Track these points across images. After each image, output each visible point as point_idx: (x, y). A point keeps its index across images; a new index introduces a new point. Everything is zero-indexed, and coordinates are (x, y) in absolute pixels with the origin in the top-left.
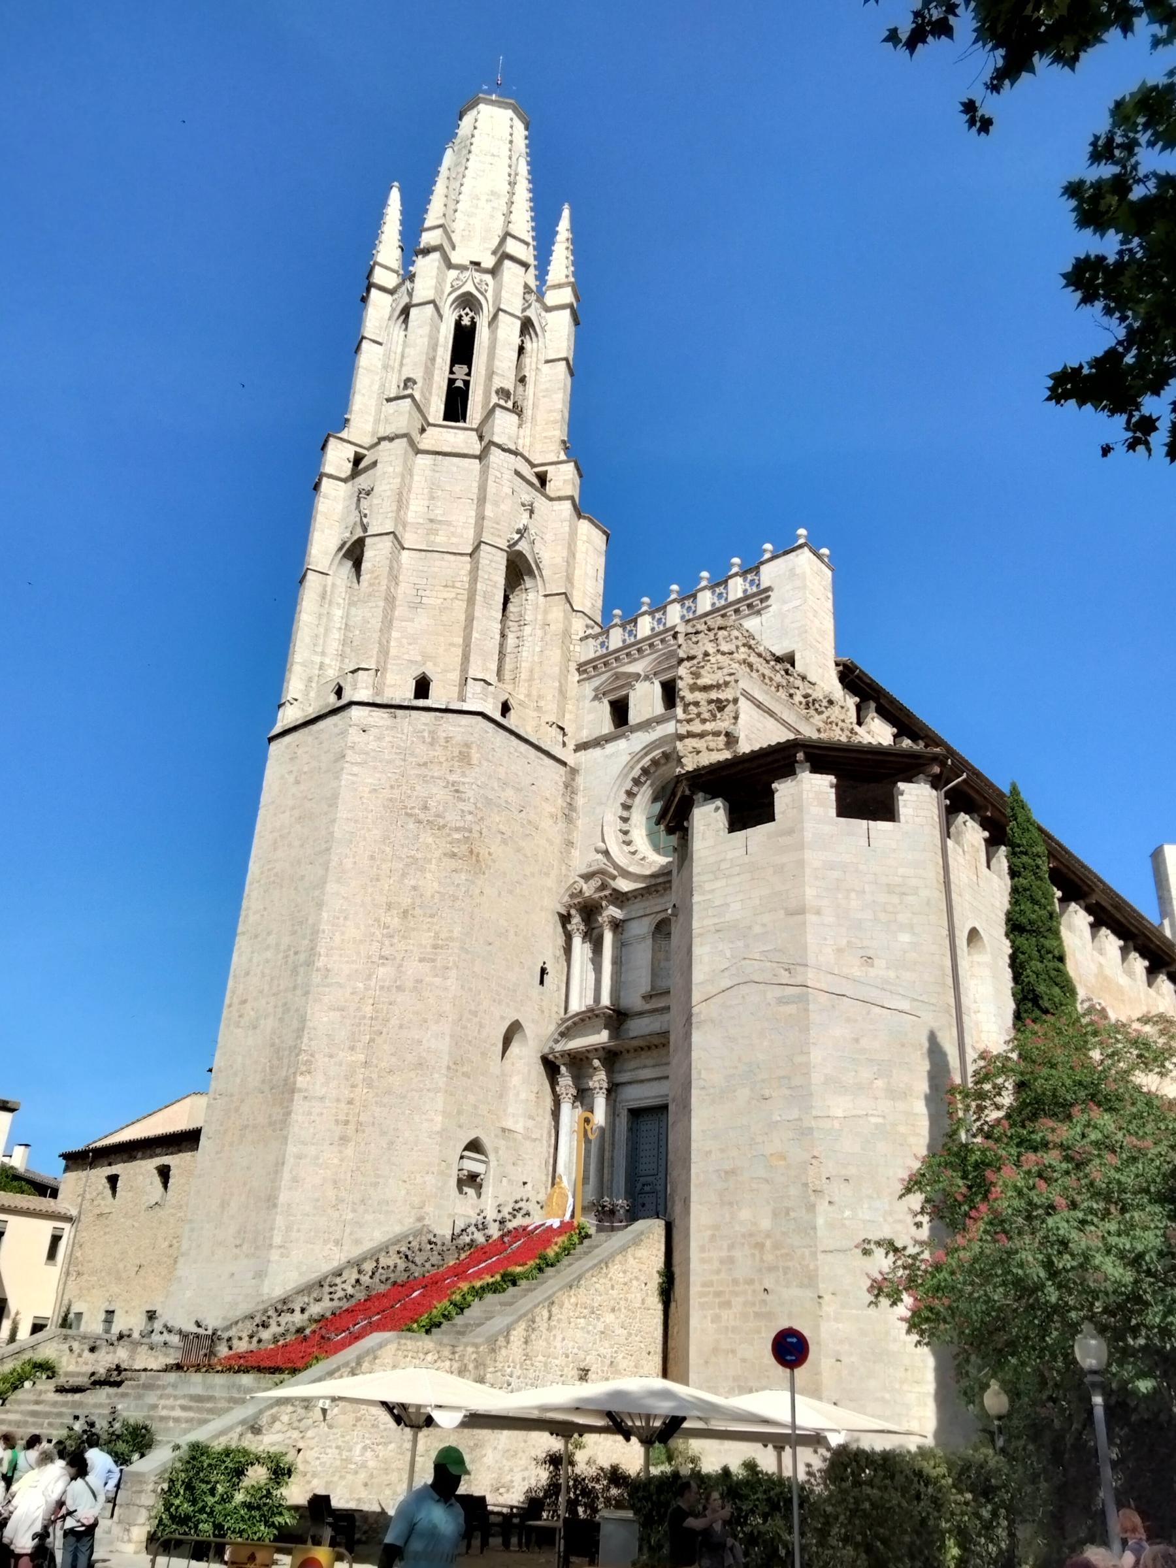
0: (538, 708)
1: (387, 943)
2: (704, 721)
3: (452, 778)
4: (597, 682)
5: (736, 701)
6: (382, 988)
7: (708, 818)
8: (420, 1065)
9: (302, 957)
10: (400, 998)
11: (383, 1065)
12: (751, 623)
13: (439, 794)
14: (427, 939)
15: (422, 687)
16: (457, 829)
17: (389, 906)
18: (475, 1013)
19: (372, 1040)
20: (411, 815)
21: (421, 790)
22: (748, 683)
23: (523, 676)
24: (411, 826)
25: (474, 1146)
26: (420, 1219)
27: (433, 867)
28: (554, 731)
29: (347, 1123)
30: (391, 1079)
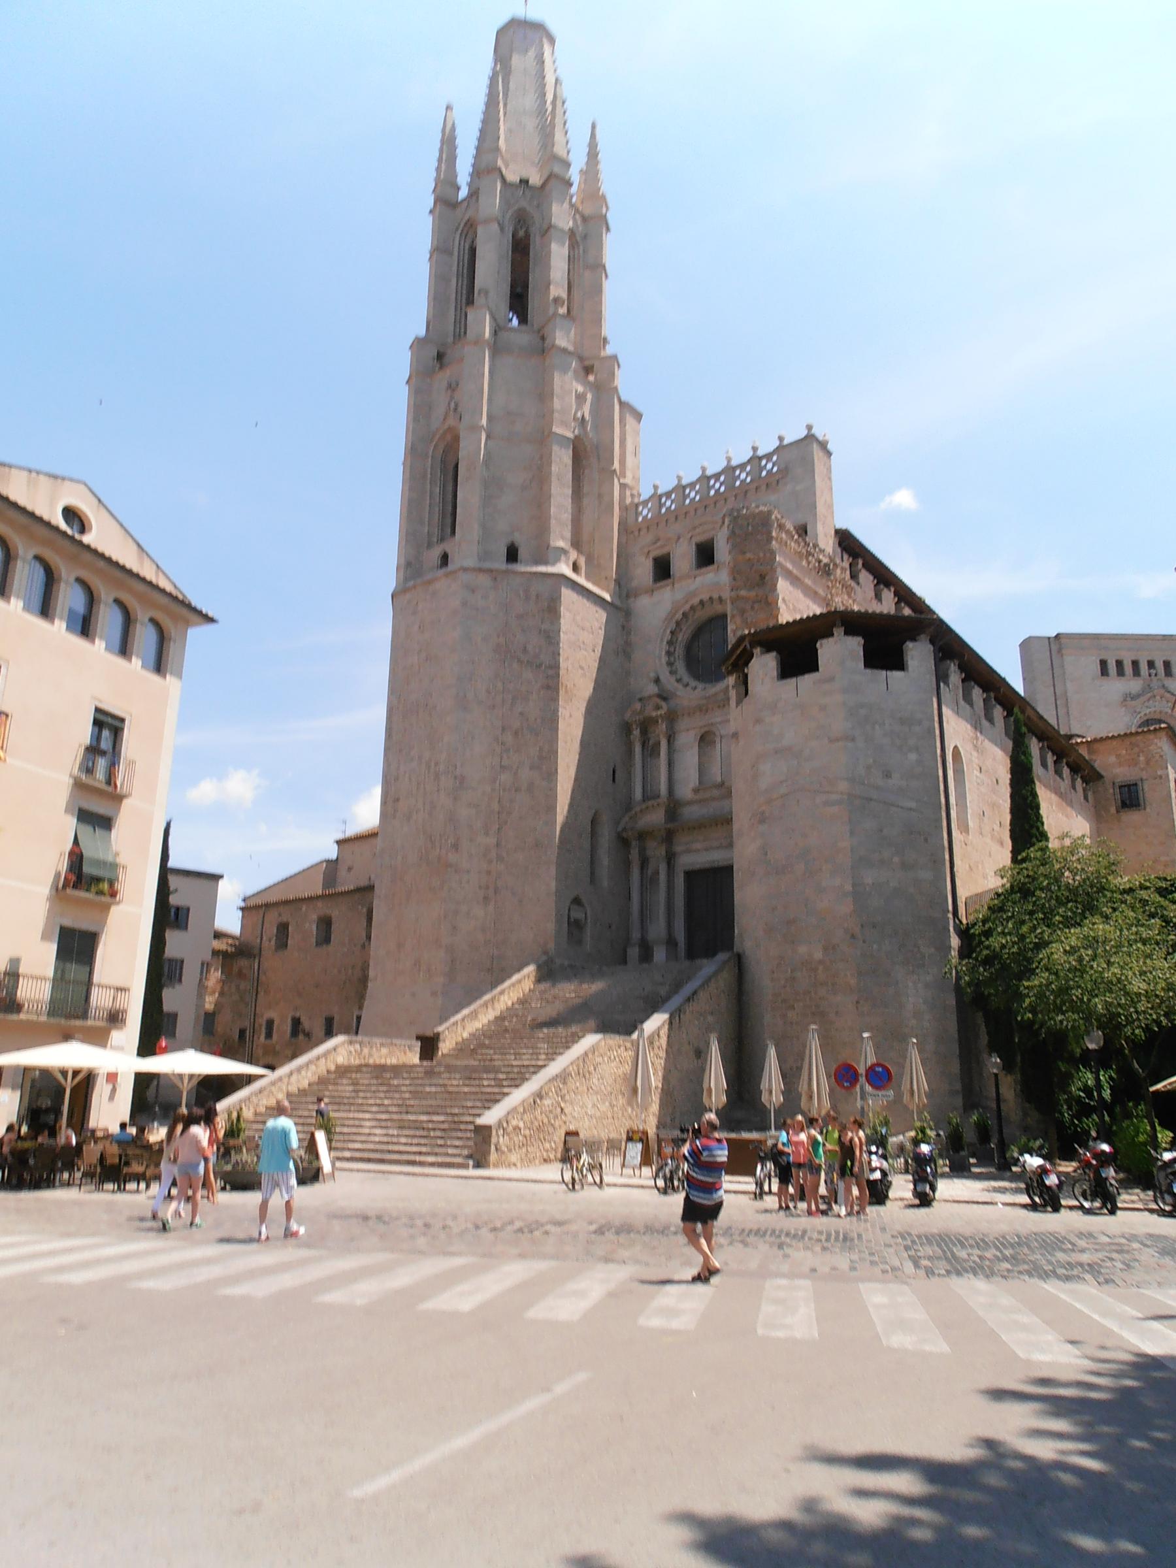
1: (505, 756)
3: (543, 627)
6: (504, 790)
9: (442, 767)
12: (773, 498)
15: (512, 555)
16: (550, 667)
17: (503, 729)
24: (515, 665)
25: (577, 901)
26: (545, 953)
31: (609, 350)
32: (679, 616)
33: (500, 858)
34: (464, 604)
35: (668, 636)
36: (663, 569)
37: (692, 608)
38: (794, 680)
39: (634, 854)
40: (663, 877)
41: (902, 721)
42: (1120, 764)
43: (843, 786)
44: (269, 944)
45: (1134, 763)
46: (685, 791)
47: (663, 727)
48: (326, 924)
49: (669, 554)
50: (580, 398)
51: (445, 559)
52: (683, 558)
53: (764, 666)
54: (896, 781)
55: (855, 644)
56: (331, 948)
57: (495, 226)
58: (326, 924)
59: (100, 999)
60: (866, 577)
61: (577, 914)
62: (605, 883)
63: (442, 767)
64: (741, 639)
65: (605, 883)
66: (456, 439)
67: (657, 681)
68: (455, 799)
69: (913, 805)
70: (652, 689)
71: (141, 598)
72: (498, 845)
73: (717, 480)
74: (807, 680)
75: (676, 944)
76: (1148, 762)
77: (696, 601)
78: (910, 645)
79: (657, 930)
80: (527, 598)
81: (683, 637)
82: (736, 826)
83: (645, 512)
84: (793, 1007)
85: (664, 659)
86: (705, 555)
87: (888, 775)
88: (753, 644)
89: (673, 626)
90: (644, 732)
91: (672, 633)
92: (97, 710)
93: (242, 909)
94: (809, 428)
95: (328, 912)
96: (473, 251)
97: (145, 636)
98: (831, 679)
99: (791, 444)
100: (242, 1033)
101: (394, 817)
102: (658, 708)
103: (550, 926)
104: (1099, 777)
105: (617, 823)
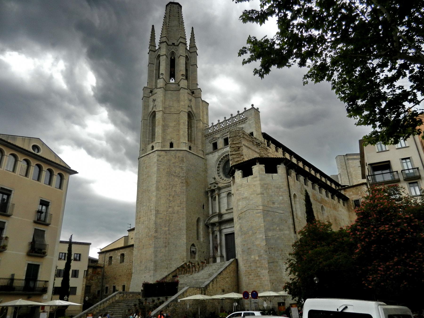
0: (197, 147)
2: (236, 151)
3: (181, 165)
4: (210, 139)
7: (238, 174)
8: (180, 229)
9: (152, 208)
10: (174, 215)
11: (172, 230)
12: (243, 126)
13: (178, 170)
14: (178, 202)
15: (171, 145)
16: (183, 177)
17: (170, 195)
18: (190, 217)
19: (169, 225)
21: (174, 169)
22: (244, 142)
23: (193, 139)
24: (172, 177)
25: (193, 245)
27: (178, 186)
28: (201, 152)
29: (166, 243)
30: (174, 233)
31: (199, 87)
32: (220, 160)
33: (169, 234)
34: (158, 160)
35: (217, 166)
37: (224, 157)
38: (246, 178)
39: (210, 229)
41: (277, 188)
42: (354, 195)
43: (261, 208)
44: (106, 264)
45: (357, 194)
46: (223, 211)
48: (123, 255)
49: (216, 142)
50: (190, 100)
51: (153, 147)
53: (238, 174)
54: (276, 205)
55: (262, 167)
56: (124, 264)
57: (165, 56)
58: (123, 255)
59: (39, 285)
60: (273, 146)
62: (202, 239)
63: (152, 208)
64: (232, 167)
66: (155, 114)
67: (215, 179)
68: (156, 217)
69: (282, 212)
70: (213, 181)
71: (56, 167)
72: (169, 230)
74: (250, 177)
75: (223, 257)
76: (361, 193)
77: (224, 155)
78: (278, 166)
80: (176, 158)
81: (221, 166)
82: (234, 221)
83: (210, 131)
84: (251, 275)
85: (217, 172)
86: (226, 142)
87: (274, 203)
88: (235, 168)
89: (218, 163)
90: (211, 194)
91: (219, 164)
92: (41, 200)
93: (99, 253)
94: (252, 105)
95: (123, 252)
96: (159, 62)
97: (56, 179)
98: (256, 177)
99: (248, 110)
100: (99, 291)
101: (139, 223)
102: (215, 186)
103: (185, 254)
104: (348, 199)
105: (205, 221)
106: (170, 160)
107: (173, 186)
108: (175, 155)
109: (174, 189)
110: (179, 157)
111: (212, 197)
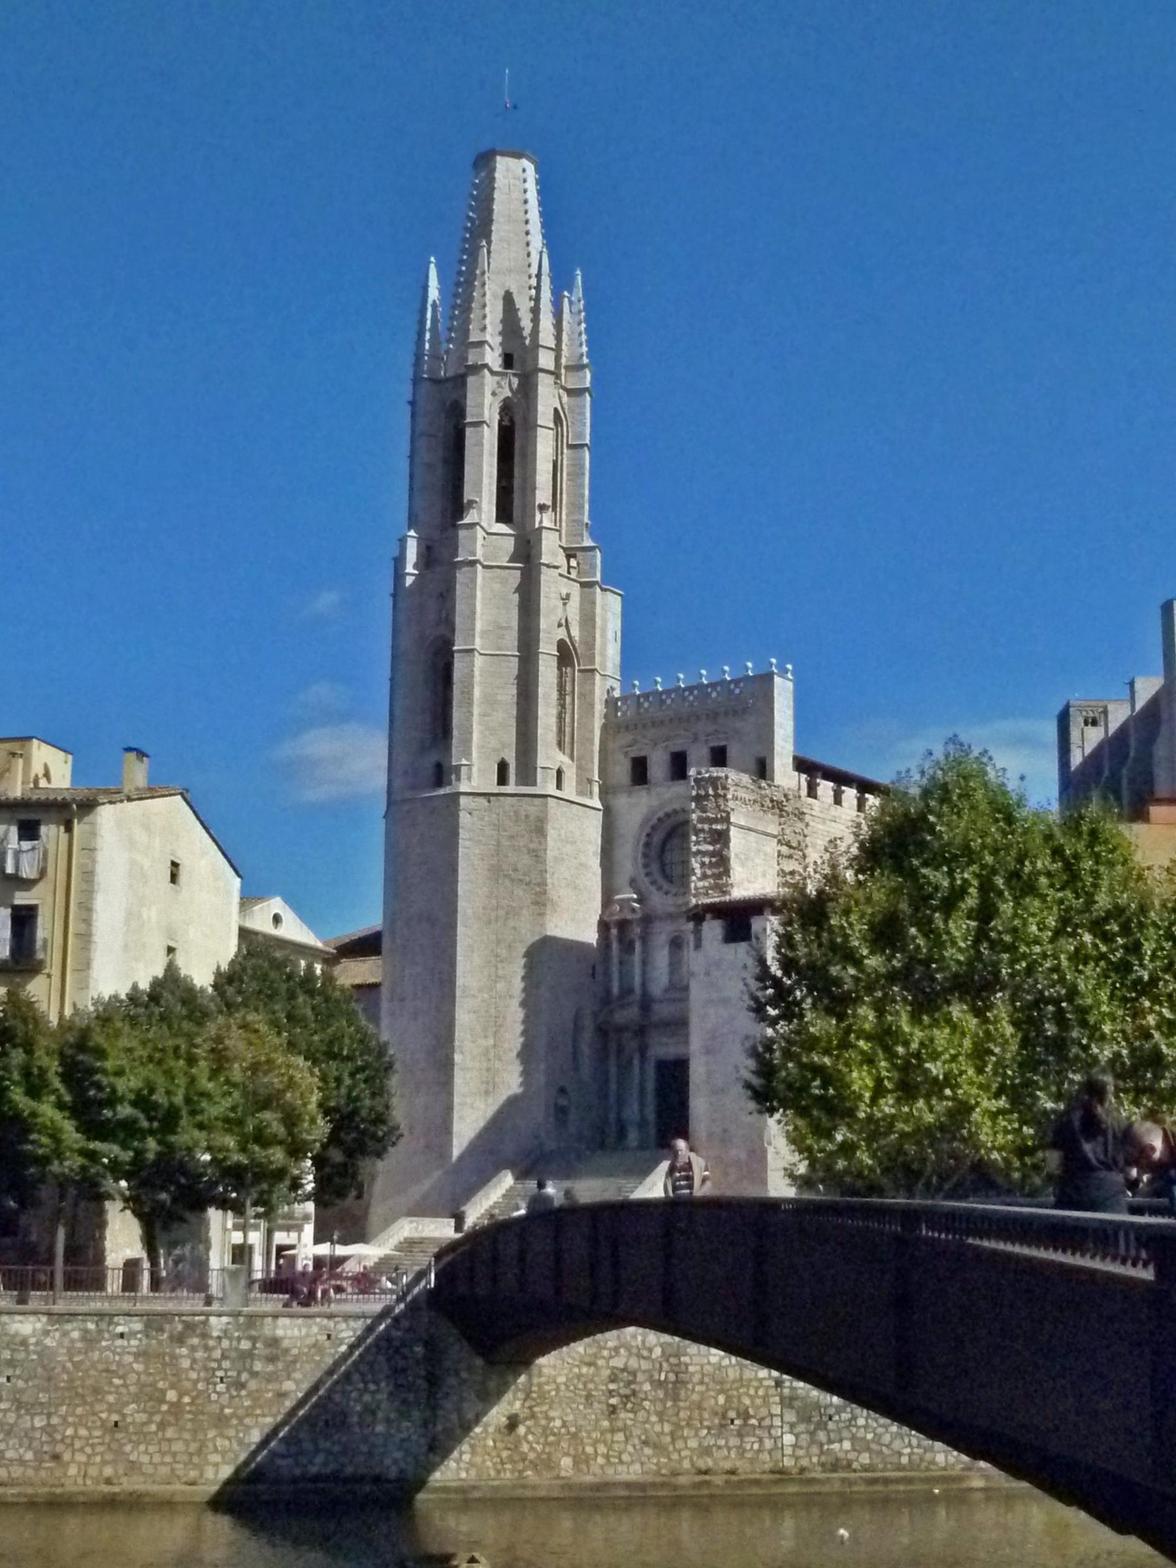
3: (532, 846)
5: (728, 830)
12: (739, 724)
13: (526, 860)
15: (503, 767)
16: (539, 885)
17: (499, 942)
20: (506, 876)
24: (507, 882)
25: (562, 1091)
27: (525, 912)
32: (654, 821)
36: (640, 772)
40: (636, 1062)
47: (638, 930)
52: (658, 767)
60: (826, 787)
61: (563, 1102)
65: (586, 1071)
73: (691, 693)
79: (632, 1111)
89: (648, 830)
91: (648, 835)
106: (498, 827)
107: (507, 913)
108: (516, 813)
109: (511, 923)
110: (527, 816)
111: (621, 940)
